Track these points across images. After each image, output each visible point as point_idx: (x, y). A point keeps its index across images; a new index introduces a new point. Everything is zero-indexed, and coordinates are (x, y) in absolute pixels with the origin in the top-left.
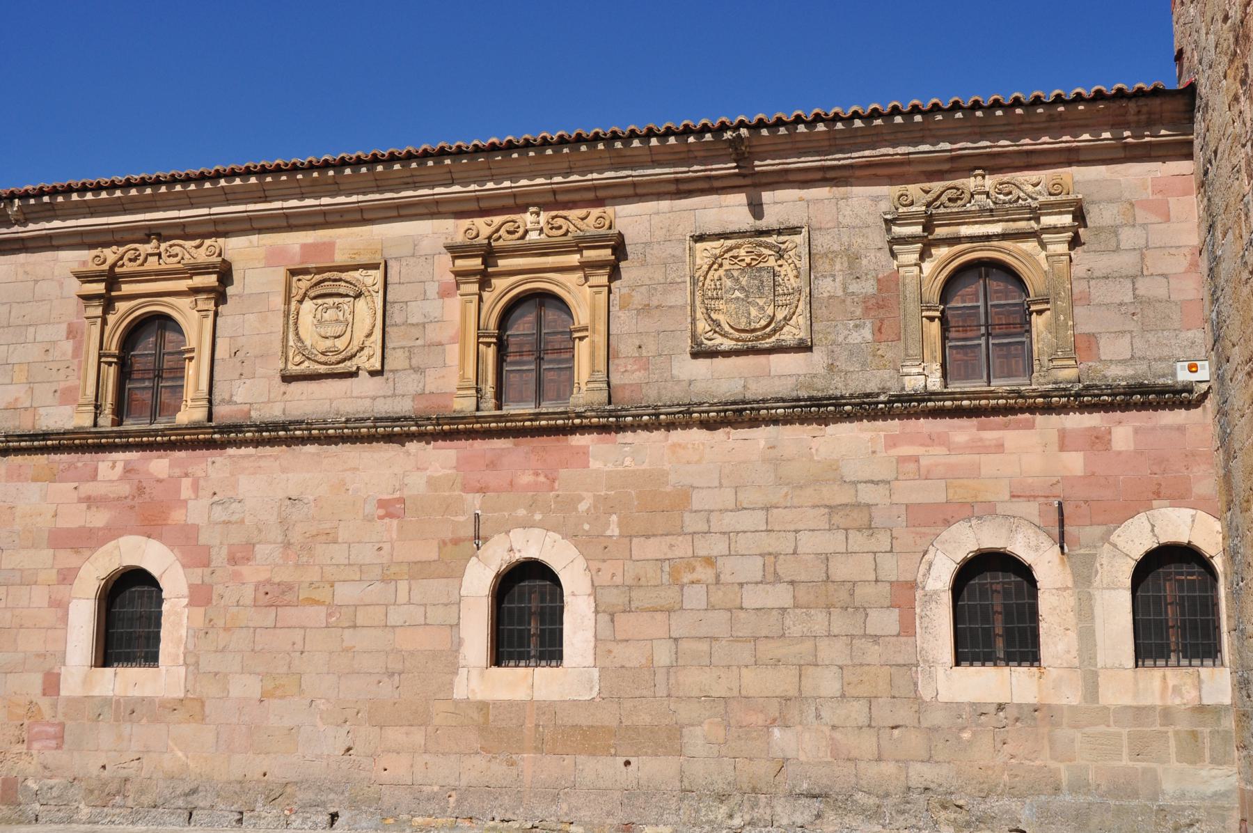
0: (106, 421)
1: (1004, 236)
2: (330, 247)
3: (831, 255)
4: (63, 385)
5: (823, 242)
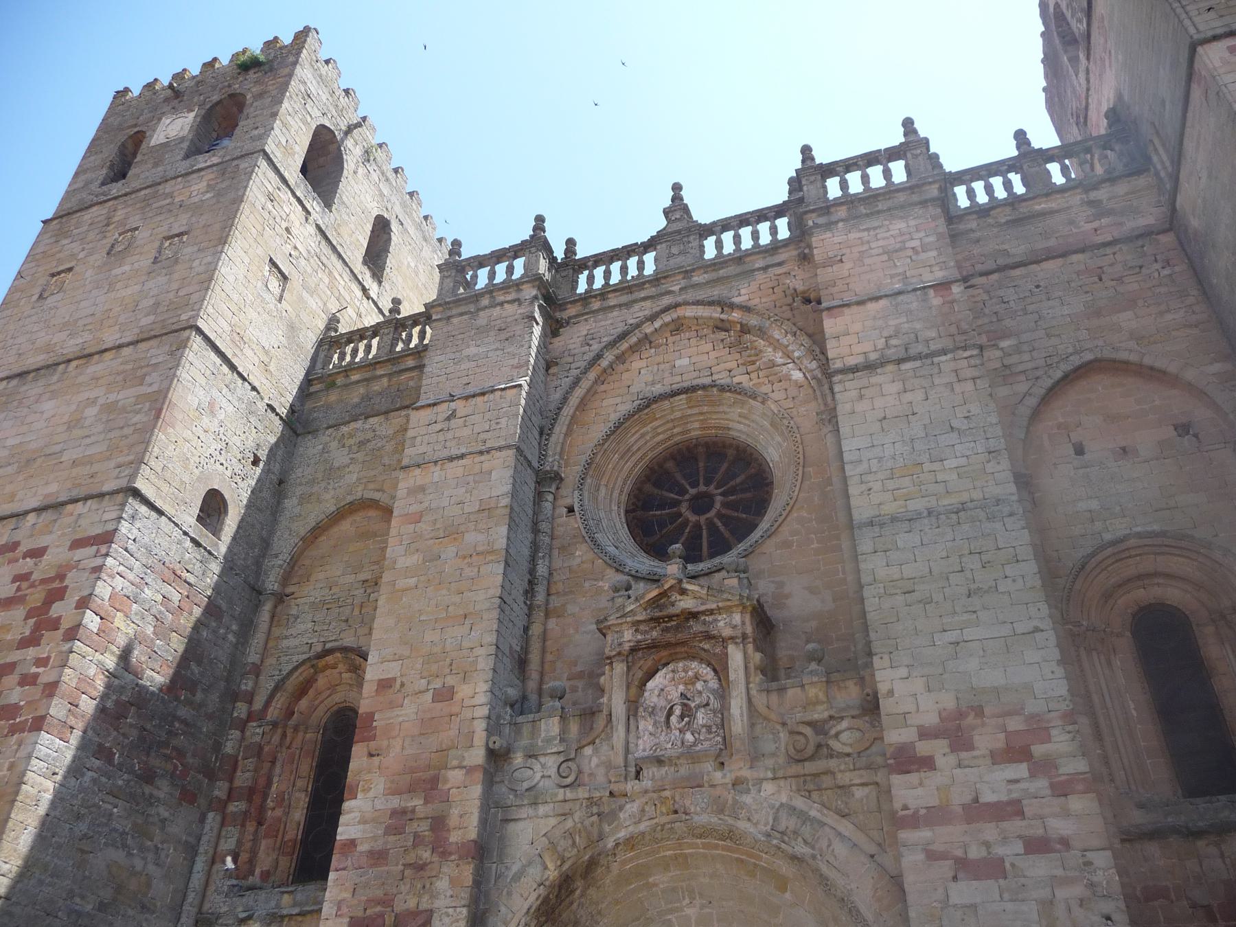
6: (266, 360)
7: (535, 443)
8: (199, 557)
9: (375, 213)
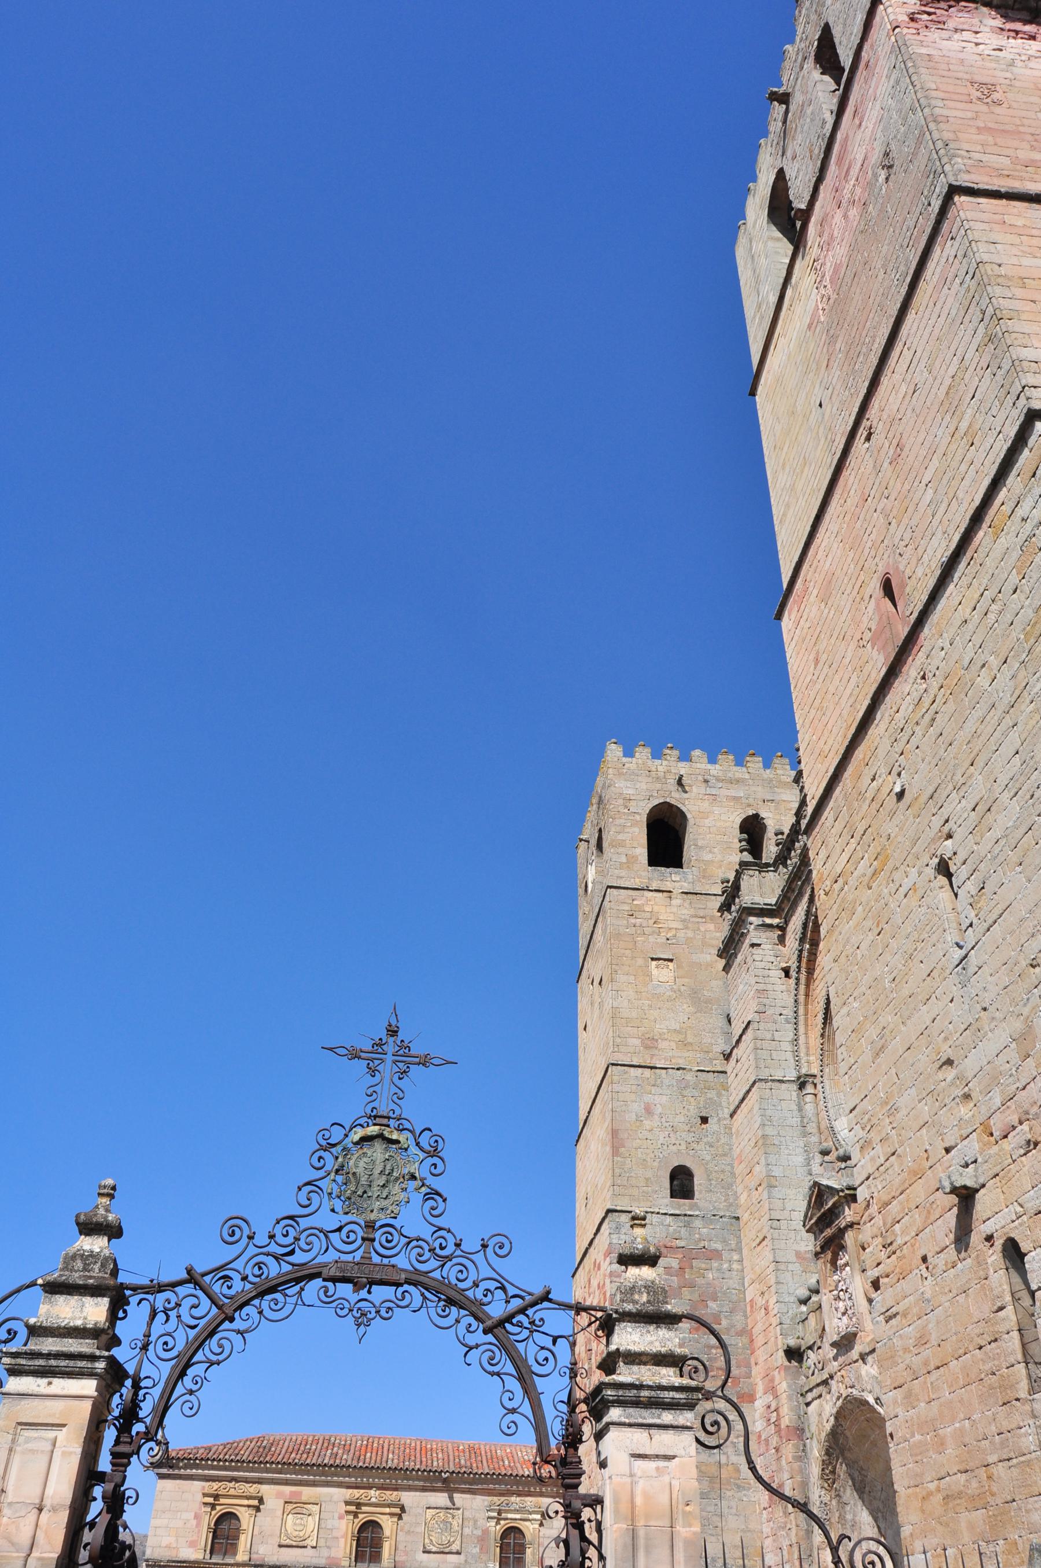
0: (208, 1556)
1: (521, 1520)
2: (300, 1493)
3: (469, 1519)
4: (191, 1539)
5: (467, 1514)
6: (681, 1037)
7: (789, 1056)
8: (681, 1224)
9: (738, 821)
